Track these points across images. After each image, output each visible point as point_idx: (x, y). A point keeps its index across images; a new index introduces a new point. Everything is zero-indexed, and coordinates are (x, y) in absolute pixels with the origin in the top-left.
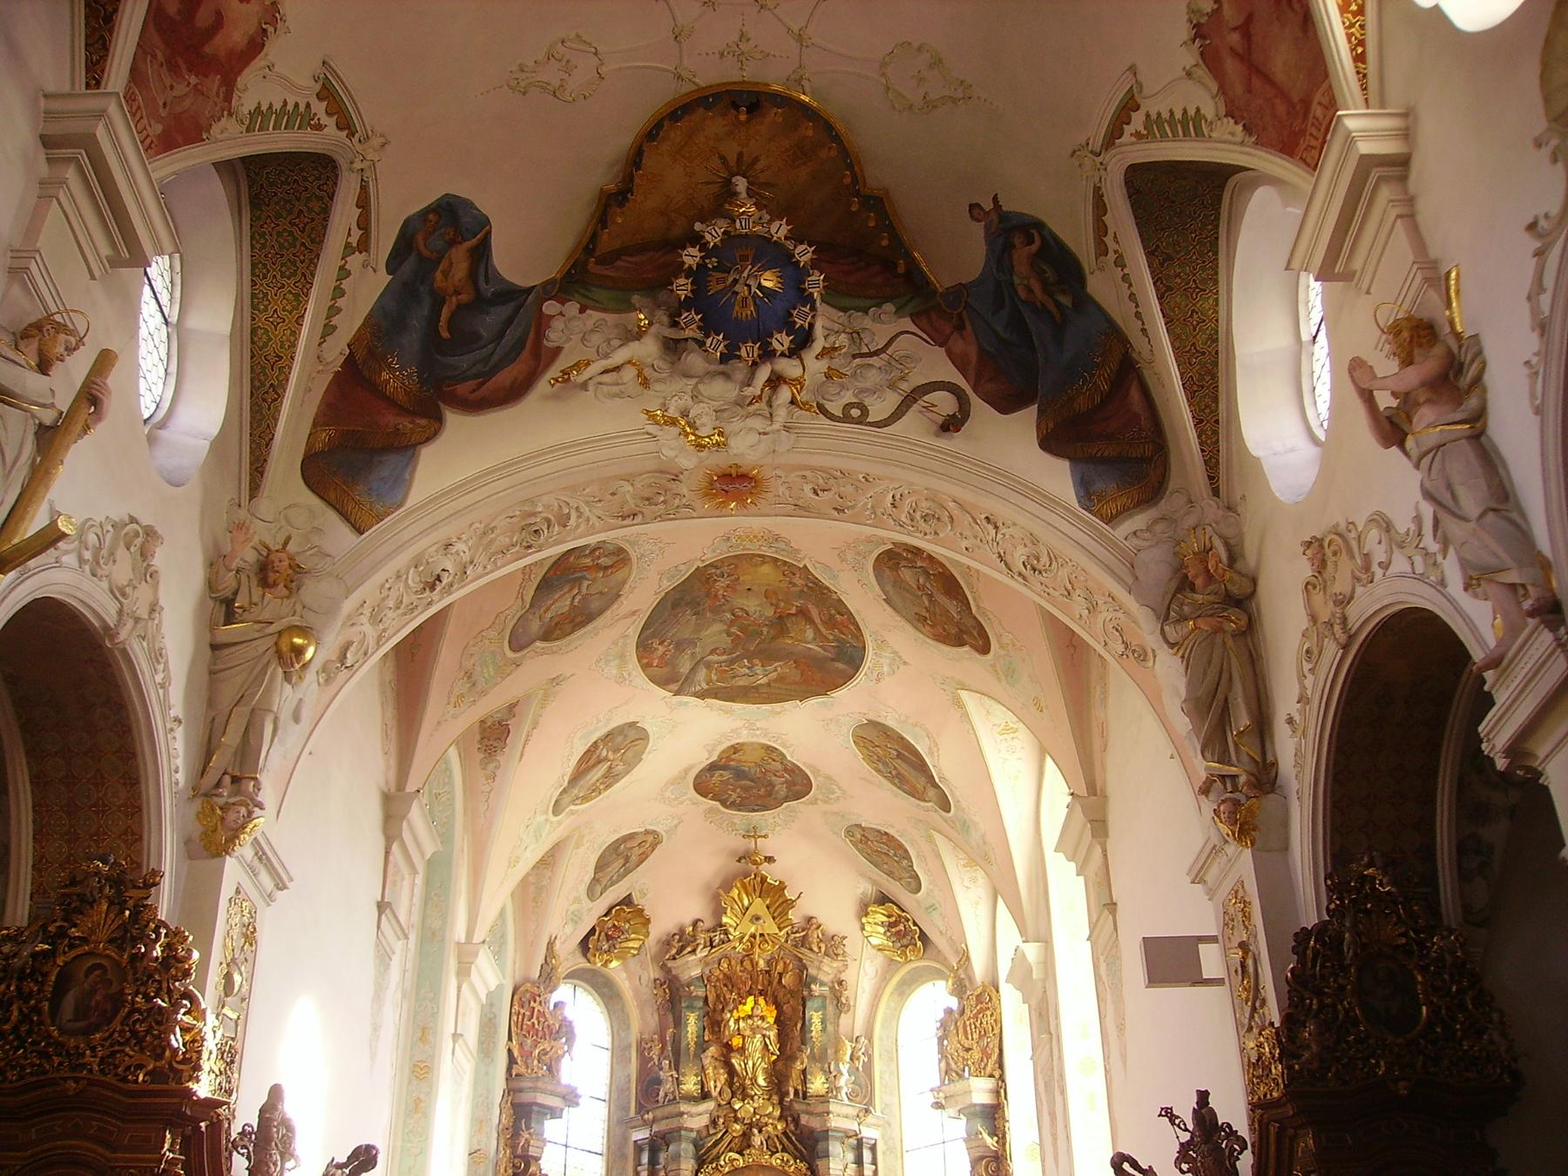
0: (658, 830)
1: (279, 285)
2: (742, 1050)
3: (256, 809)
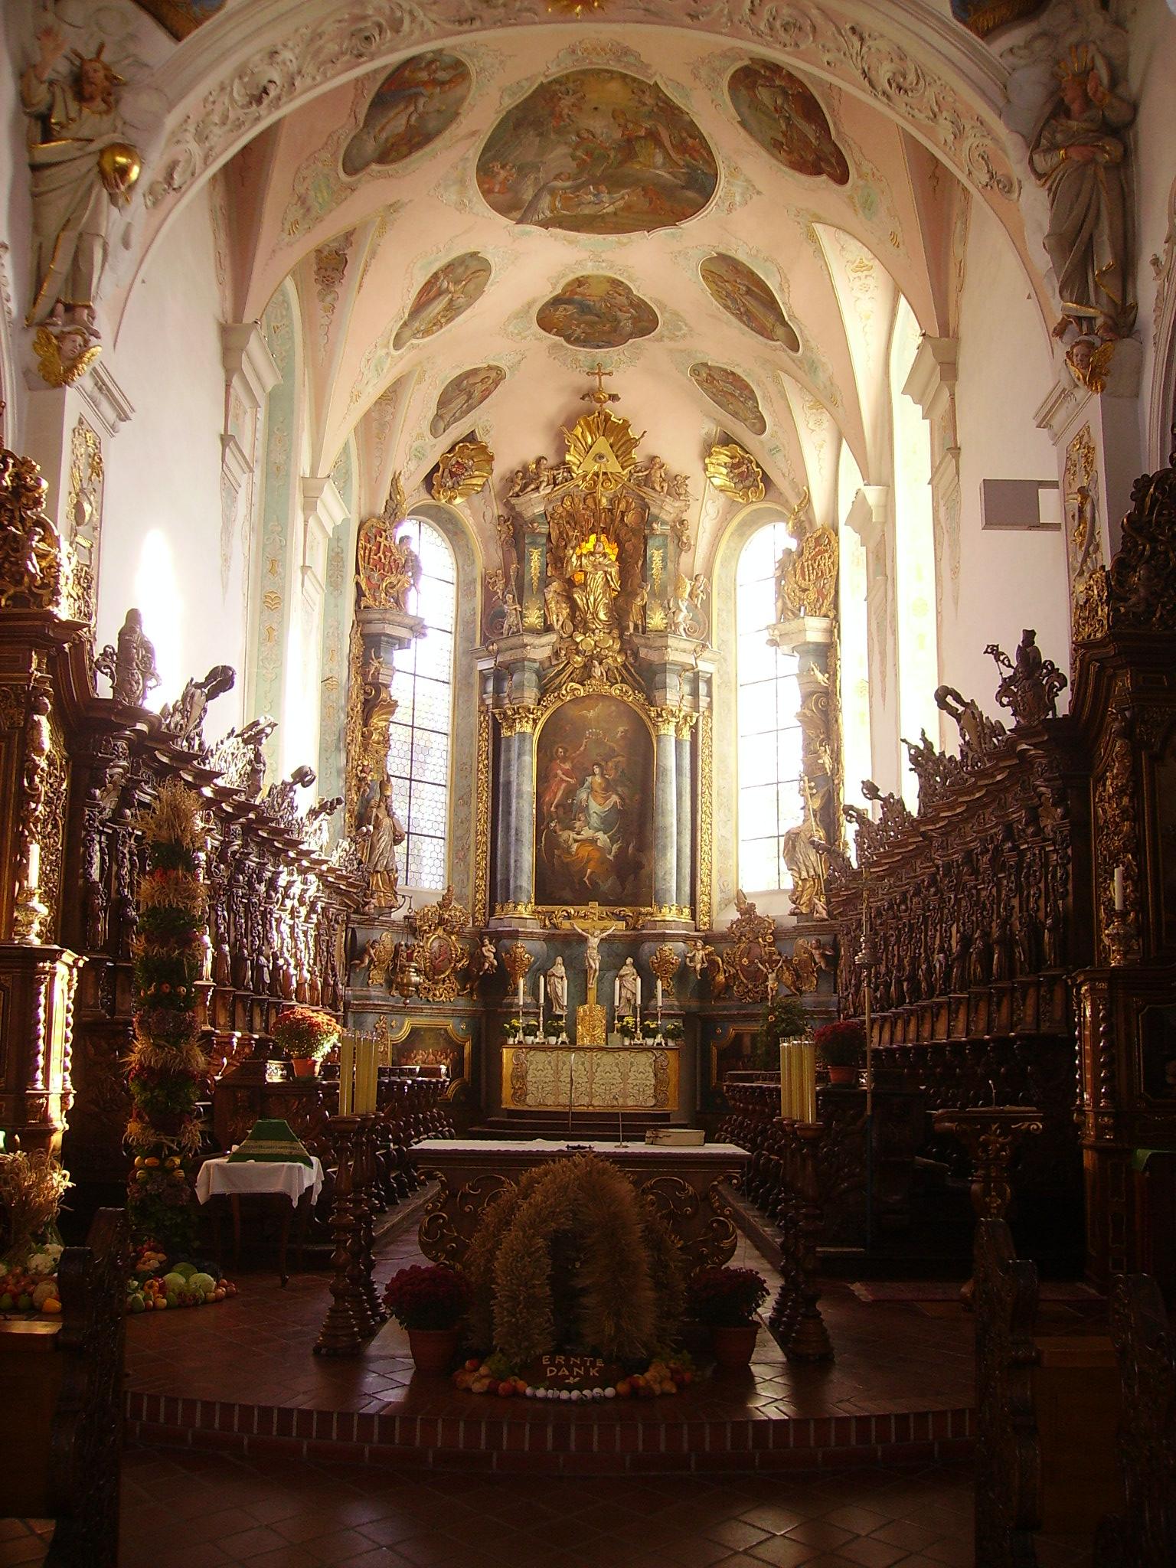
2: (584, 586)
3: (92, 338)
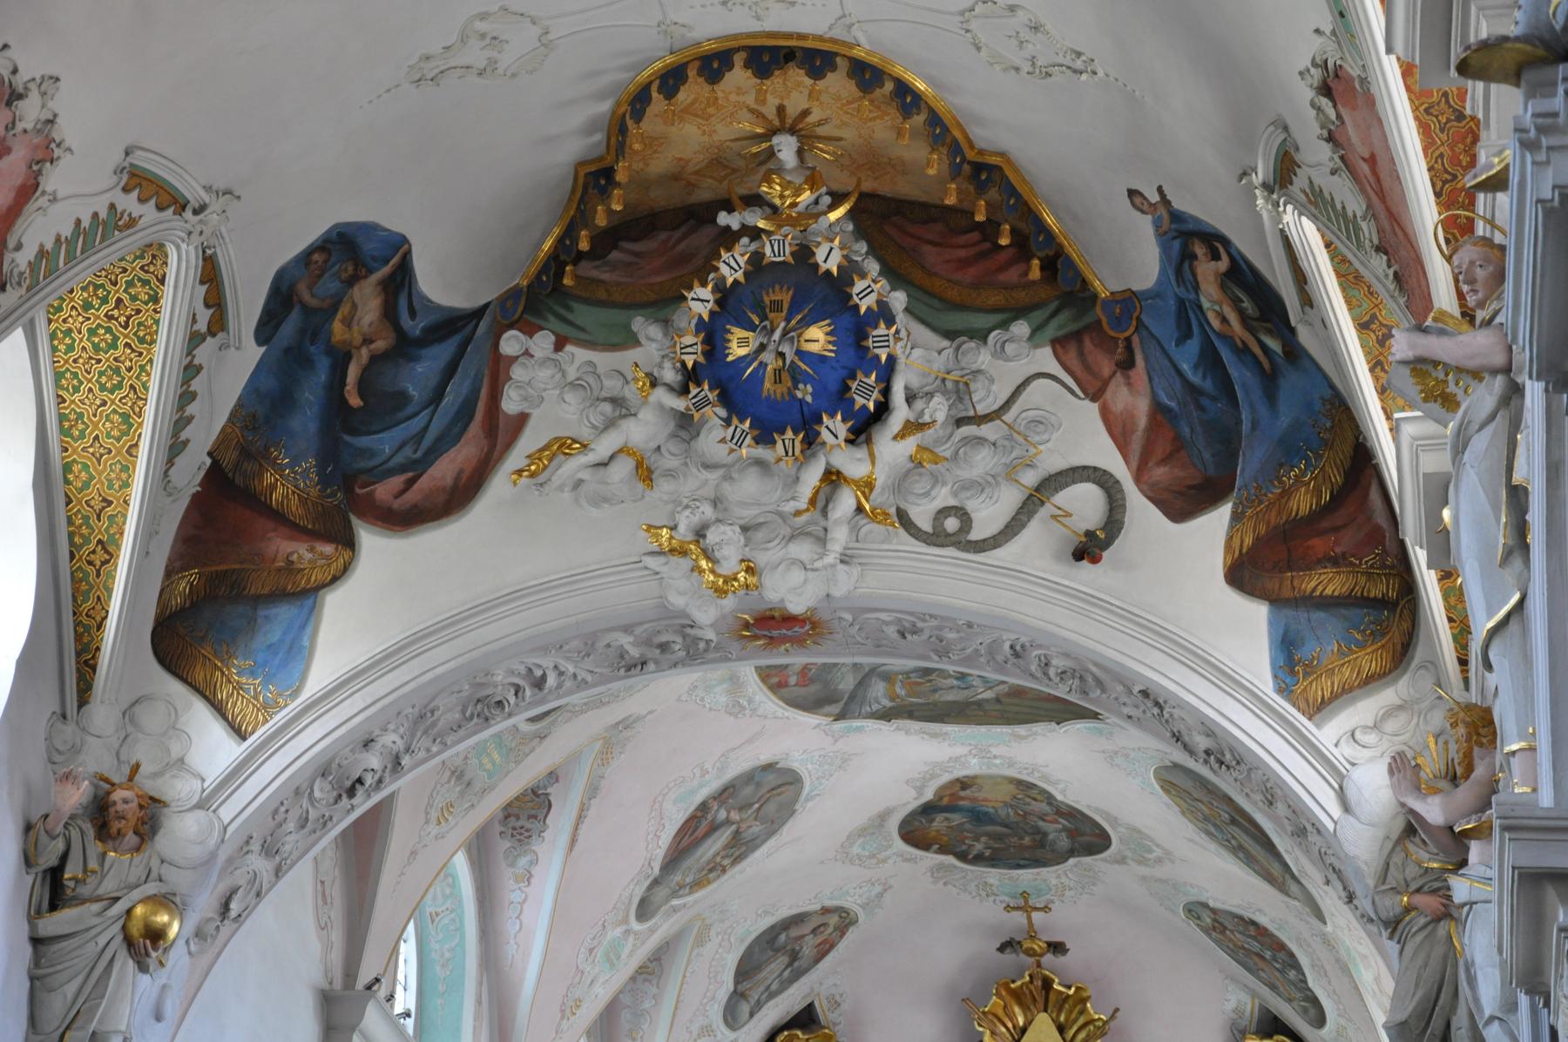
0: (846, 905)
1: (98, 402)
